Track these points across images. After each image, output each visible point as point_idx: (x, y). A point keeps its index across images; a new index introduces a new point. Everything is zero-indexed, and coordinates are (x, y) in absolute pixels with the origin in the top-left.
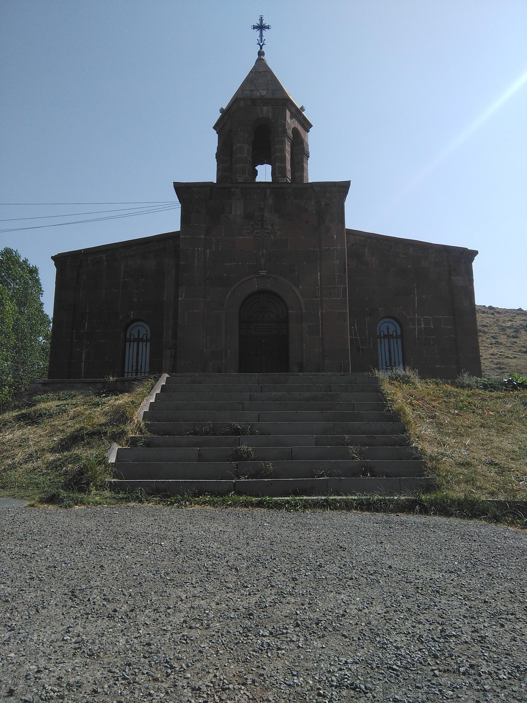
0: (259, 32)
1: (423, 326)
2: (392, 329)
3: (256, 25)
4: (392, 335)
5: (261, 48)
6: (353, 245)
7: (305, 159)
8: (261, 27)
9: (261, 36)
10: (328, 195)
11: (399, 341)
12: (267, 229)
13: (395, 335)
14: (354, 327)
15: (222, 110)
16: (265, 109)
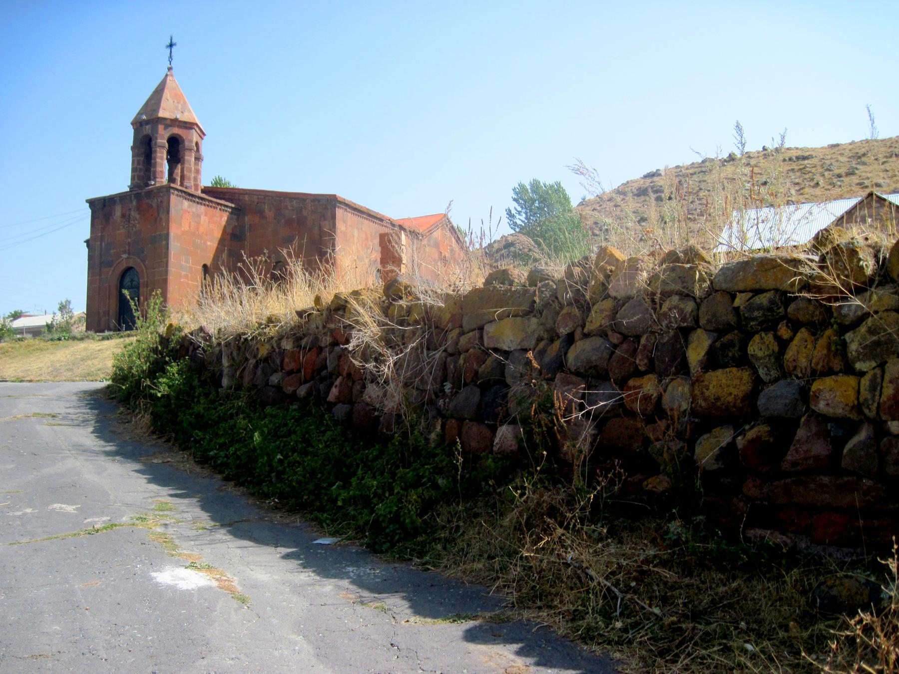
8: (171, 45)
10: (161, 194)
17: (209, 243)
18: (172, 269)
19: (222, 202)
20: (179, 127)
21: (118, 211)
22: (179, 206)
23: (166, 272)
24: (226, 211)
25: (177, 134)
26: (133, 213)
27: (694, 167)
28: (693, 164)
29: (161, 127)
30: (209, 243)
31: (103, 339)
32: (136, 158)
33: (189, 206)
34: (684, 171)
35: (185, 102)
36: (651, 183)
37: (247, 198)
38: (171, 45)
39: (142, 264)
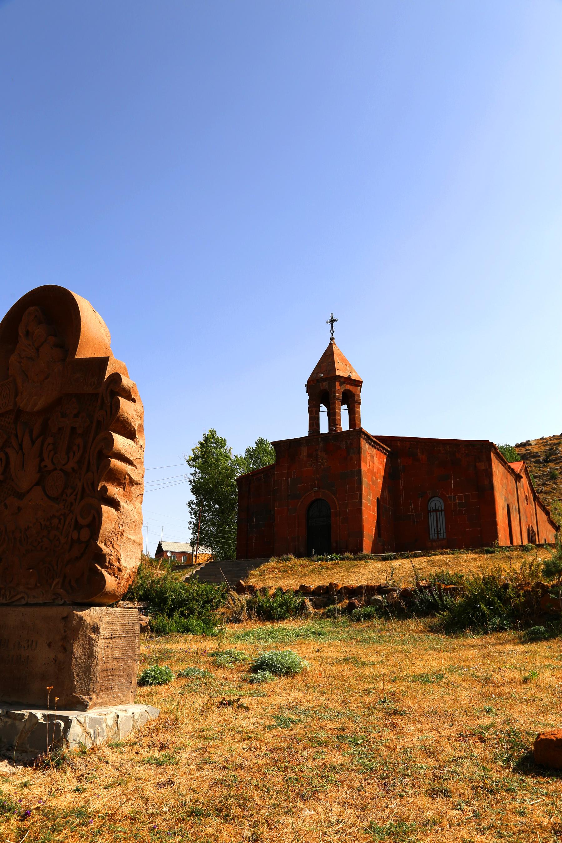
0: (331, 324)
1: (457, 501)
2: (438, 505)
3: (329, 320)
4: (439, 509)
5: (332, 336)
6: (409, 448)
7: (356, 406)
8: (332, 321)
9: (332, 327)
10: (351, 437)
11: (443, 513)
12: (320, 462)
13: (440, 509)
14: (411, 506)
15: (306, 385)
16: (324, 384)
17: (379, 480)
18: (364, 501)
19: (385, 446)
20: (350, 384)
21: (304, 452)
22: (365, 447)
23: (360, 503)
24: (386, 454)
25: (349, 391)
26: (319, 453)
27: (557, 439)
28: (554, 436)
29: (337, 384)
30: (379, 480)
31: (385, 559)
32: (314, 409)
33: (369, 448)
34: (550, 442)
35: (350, 366)
36: (526, 450)
37: (399, 444)
38: (332, 321)
39: (334, 497)
